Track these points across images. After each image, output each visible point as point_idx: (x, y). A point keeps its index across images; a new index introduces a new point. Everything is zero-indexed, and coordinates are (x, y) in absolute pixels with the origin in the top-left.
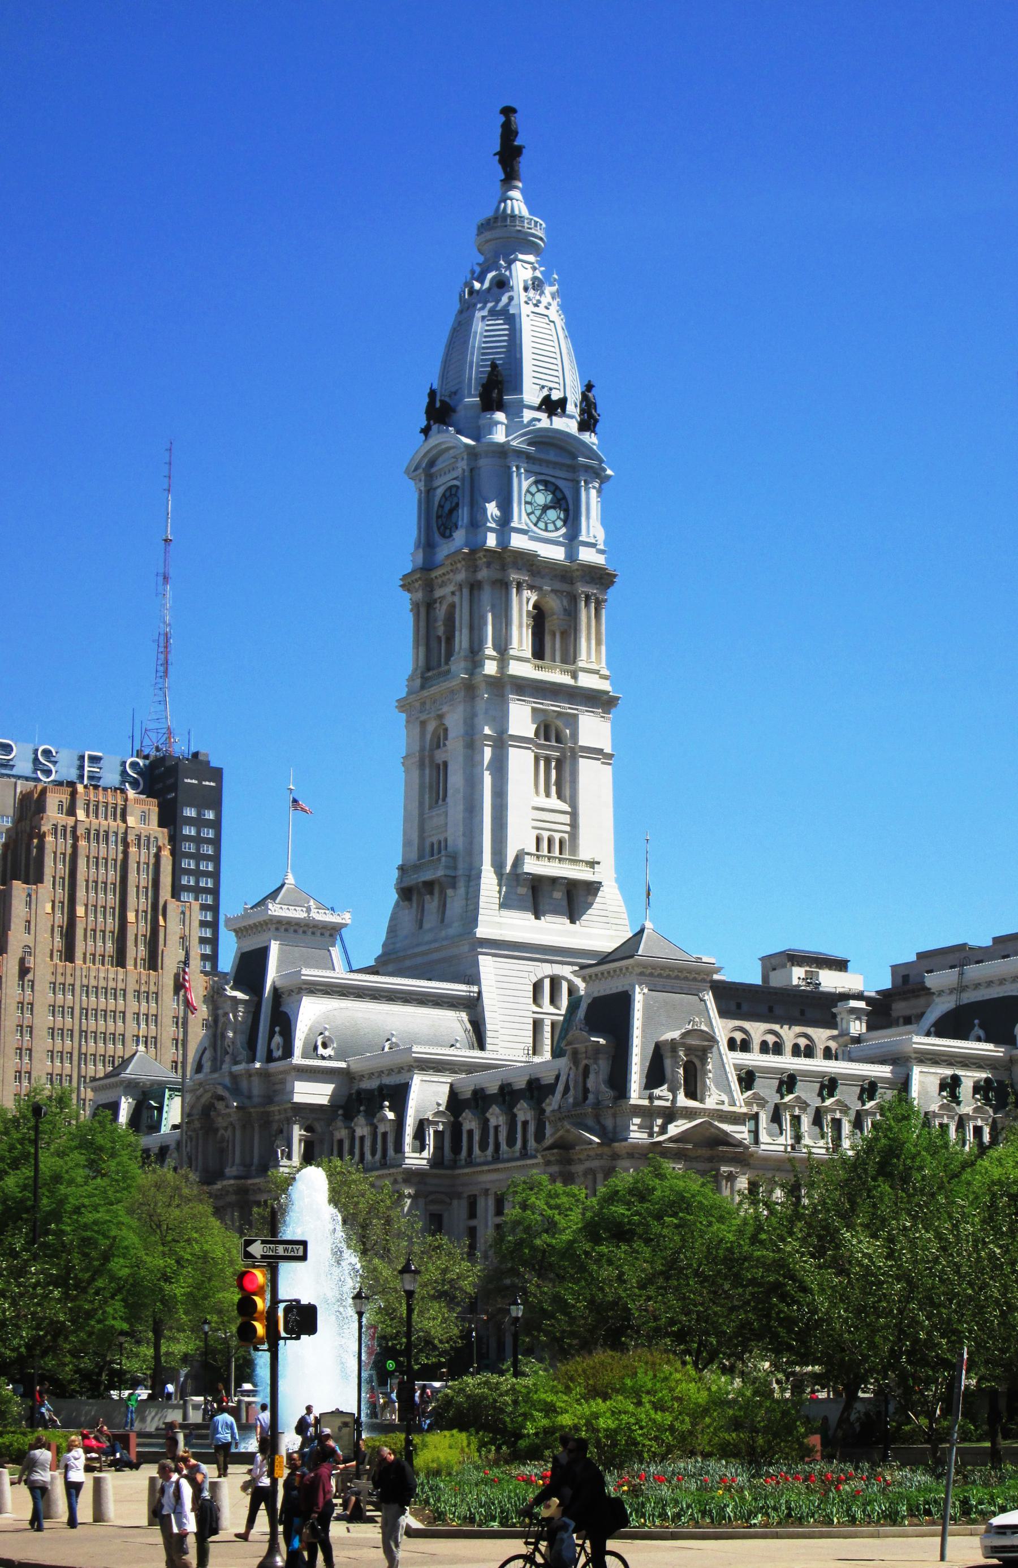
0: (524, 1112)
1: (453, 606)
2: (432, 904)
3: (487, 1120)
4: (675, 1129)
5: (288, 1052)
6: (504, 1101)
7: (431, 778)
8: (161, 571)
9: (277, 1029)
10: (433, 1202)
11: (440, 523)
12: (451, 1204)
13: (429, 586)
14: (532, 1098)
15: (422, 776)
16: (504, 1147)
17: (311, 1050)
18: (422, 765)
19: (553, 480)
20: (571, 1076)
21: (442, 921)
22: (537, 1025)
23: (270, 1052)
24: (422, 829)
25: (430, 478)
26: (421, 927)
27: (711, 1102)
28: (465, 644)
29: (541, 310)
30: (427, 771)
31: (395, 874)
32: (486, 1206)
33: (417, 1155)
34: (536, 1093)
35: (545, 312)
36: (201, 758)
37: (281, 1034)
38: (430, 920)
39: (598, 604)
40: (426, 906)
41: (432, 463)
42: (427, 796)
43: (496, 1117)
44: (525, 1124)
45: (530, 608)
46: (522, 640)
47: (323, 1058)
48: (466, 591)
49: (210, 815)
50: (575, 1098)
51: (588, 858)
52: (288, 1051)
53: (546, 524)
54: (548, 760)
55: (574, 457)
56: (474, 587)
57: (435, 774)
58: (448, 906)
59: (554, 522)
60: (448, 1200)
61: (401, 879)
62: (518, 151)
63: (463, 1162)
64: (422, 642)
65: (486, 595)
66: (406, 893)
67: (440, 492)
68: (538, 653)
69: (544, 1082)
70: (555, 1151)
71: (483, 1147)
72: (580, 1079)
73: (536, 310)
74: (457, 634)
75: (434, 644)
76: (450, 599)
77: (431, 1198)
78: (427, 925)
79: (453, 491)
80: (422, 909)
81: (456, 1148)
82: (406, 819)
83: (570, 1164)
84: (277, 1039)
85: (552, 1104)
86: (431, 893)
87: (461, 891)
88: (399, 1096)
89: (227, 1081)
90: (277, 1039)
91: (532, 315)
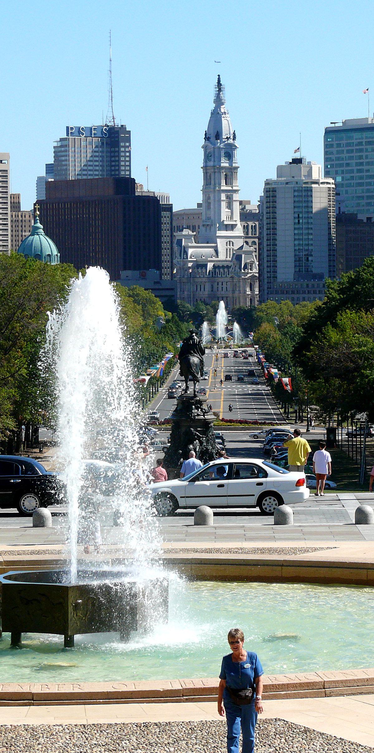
0: (226, 270)
4: (248, 276)
13: (206, 170)
17: (191, 258)
22: (227, 249)
27: (254, 271)
32: (220, 284)
36: (124, 127)
38: (208, 231)
41: (206, 147)
46: (223, 182)
49: (127, 144)
52: (187, 258)
56: (215, 172)
68: (226, 184)
84: (185, 255)
85: (230, 270)
88: (206, 266)
90: (185, 255)
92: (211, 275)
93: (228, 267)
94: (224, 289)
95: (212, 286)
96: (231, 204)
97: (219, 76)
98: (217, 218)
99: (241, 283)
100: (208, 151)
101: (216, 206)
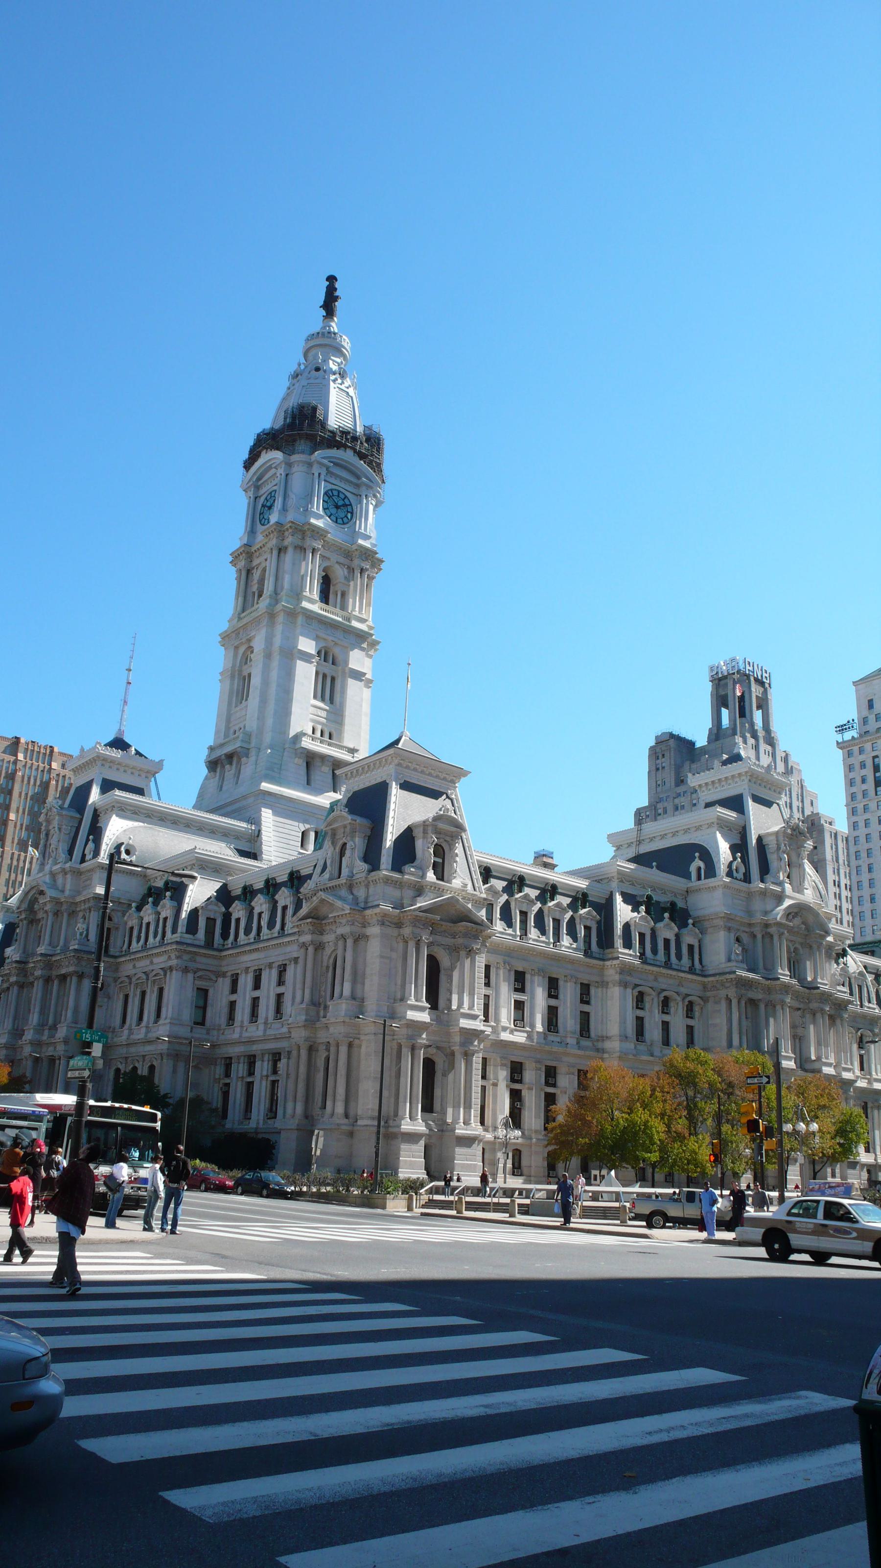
0: (284, 897)
1: (264, 570)
2: (230, 771)
3: (253, 908)
5: (96, 853)
6: (268, 892)
7: (238, 685)
8: (123, 698)
9: (91, 837)
10: (200, 977)
14: (292, 887)
15: (232, 684)
16: (265, 930)
18: (232, 677)
21: (237, 783)
23: (84, 856)
24: (228, 721)
25: (257, 488)
26: (221, 790)
29: (343, 387)
31: (206, 752)
32: (245, 982)
34: (296, 882)
35: (346, 390)
37: (94, 841)
38: (228, 784)
39: (371, 578)
41: (259, 479)
42: (234, 699)
43: (260, 904)
44: (285, 908)
45: (322, 569)
46: (312, 590)
48: (275, 552)
50: (331, 874)
51: (351, 746)
53: (337, 519)
54: (325, 676)
55: (358, 478)
56: (281, 550)
59: (342, 519)
60: (215, 979)
61: (209, 756)
62: (336, 299)
63: (230, 946)
64: (241, 594)
65: (289, 557)
66: (213, 765)
67: (262, 499)
68: (325, 597)
69: (304, 872)
70: (309, 920)
71: (247, 932)
72: (338, 858)
73: (339, 386)
74: (266, 582)
75: (250, 598)
76: (263, 565)
77: (200, 974)
78: (224, 788)
79: (273, 495)
80: (222, 778)
81: (225, 935)
82: (218, 716)
83: (322, 934)
84: (91, 845)
85: (309, 886)
86: (231, 763)
87: (253, 759)
89: (47, 879)
90: (91, 845)
91: (337, 389)
92: (201, 934)
93: (296, 879)
94: (266, 1008)
95: (203, 993)
96: (338, 683)
97: (332, 279)
98: (270, 722)
99: (374, 949)
100: (265, 490)
101: (274, 675)
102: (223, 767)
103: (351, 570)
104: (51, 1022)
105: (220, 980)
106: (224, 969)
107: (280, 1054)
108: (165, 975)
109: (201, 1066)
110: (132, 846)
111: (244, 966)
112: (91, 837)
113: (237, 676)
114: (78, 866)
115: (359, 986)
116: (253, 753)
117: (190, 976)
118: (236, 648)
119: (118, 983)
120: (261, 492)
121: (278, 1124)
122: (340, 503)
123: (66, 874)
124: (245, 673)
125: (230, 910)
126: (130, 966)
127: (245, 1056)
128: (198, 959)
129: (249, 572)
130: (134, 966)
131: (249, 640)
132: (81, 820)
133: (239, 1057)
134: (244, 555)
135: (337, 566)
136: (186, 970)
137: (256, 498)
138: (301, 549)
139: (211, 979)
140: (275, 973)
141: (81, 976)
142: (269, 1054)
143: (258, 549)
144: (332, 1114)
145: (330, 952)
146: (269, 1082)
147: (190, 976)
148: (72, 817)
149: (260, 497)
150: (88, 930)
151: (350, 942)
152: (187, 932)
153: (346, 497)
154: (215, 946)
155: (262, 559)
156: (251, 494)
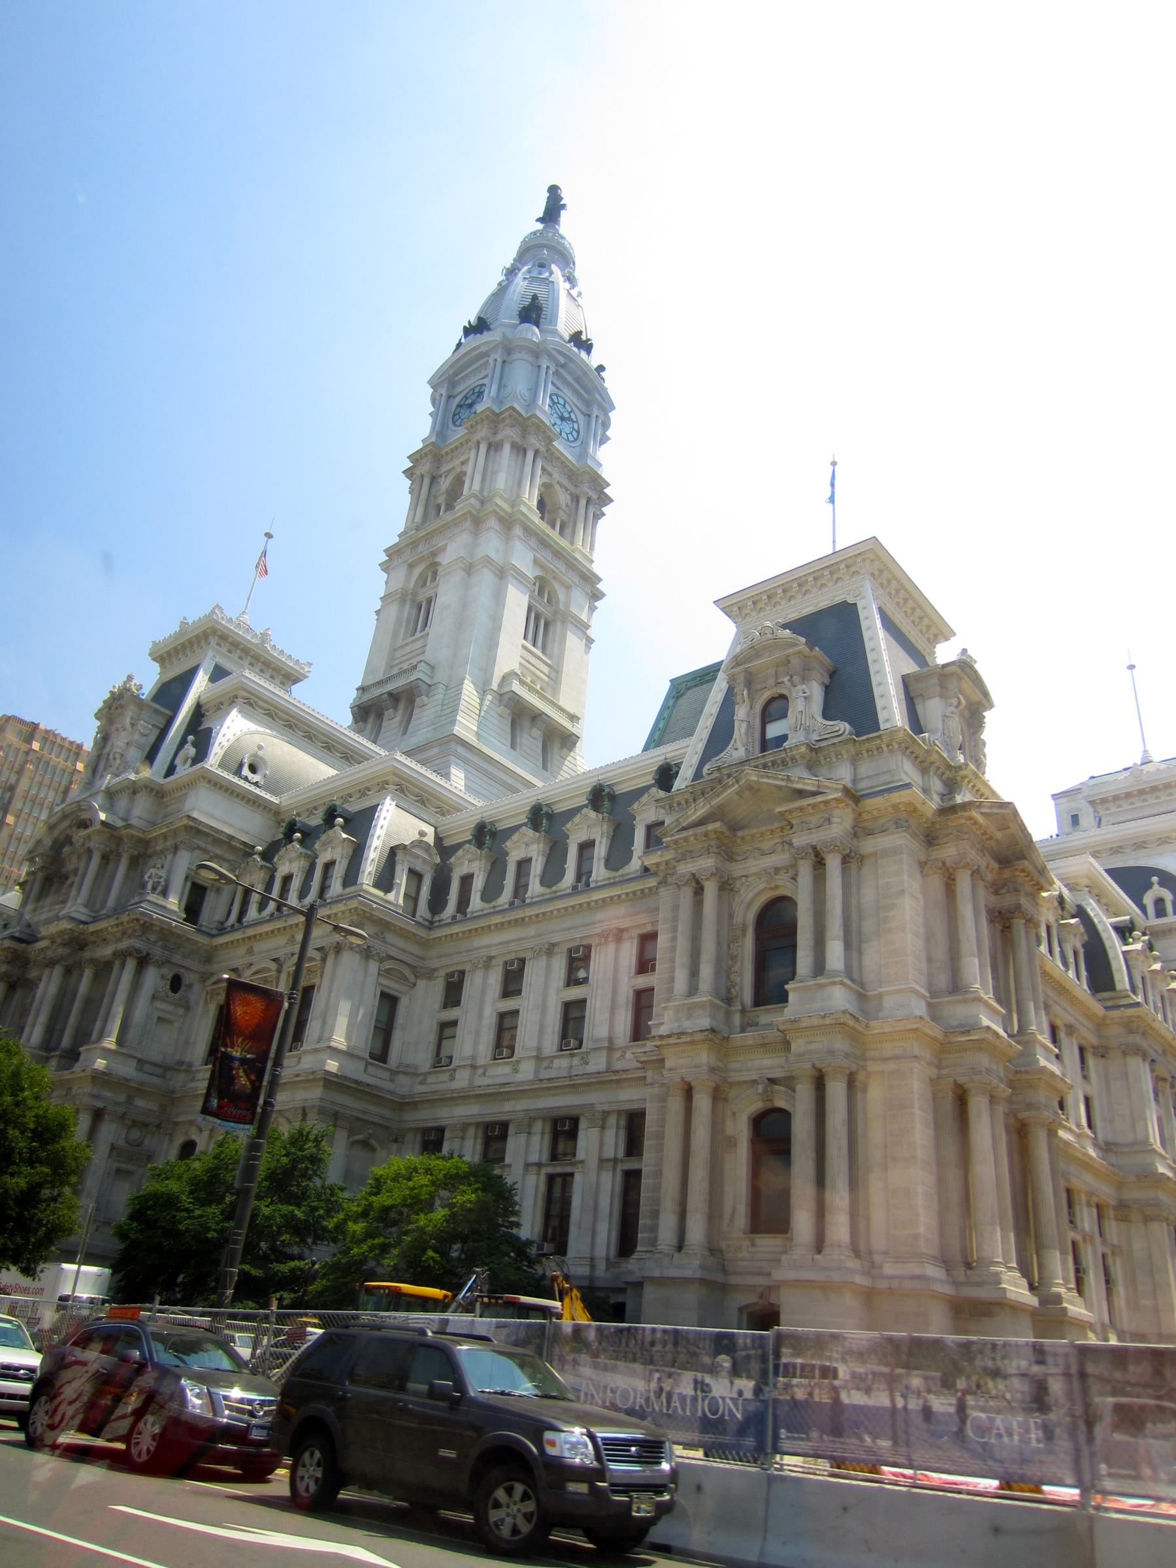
2: (392, 721)
7: (410, 613)
11: (458, 411)
12: (414, 985)
18: (403, 601)
19: (571, 403)
20: (741, 712)
21: (404, 733)
25: (453, 384)
28: (476, 486)
30: (407, 607)
31: (354, 694)
33: (380, 893)
34: (607, 803)
37: (194, 745)
40: (384, 724)
42: (402, 630)
47: (246, 779)
51: (572, 710)
56: (494, 447)
57: (414, 612)
58: (414, 717)
60: (411, 978)
67: (458, 399)
72: (757, 723)
76: (458, 470)
77: (389, 965)
81: (437, 902)
97: (554, 190)
102: (380, 716)
103: (576, 499)
104: (66, 1042)
105: (421, 984)
106: (434, 964)
107: (575, 1121)
108: (324, 960)
109: (373, 1142)
110: (261, 759)
111: (484, 953)
112: (191, 738)
113: (409, 602)
114: (161, 781)
115: (855, 954)
116: (441, 689)
117: (373, 966)
118: (411, 567)
119: (209, 982)
120: (459, 389)
121: (633, 1266)
122: (566, 415)
123: (135, 792)
124: (422, 596)
125: (452, 860)
126: (242, 950)
127: (477, 1125)
128: (390, 938)
129: (434, 480)
130: (250, 951)
131: (434, 554)
132: (170, 721)
133: (465, 1127)
134: (429, 457)
135: (557, 487)
136: (367, 953)
137: (449, 397)
138: (520, 450)
139: (406, 979)
140: (559, 965)
141: (143, 962)
142: (544, 1119)
143: (452, 451)
144: (819, 1244)
145: (750, 896)
146: (543, 1178)
147: (373, 966)
148: (157, 711)
149: (454, 397)
150: (167, 881)
151: (833, 864)
152: (376, 885)
153: (572, 411)
154: (418, 918)
155: (457, 462)
156: (444, 391)
